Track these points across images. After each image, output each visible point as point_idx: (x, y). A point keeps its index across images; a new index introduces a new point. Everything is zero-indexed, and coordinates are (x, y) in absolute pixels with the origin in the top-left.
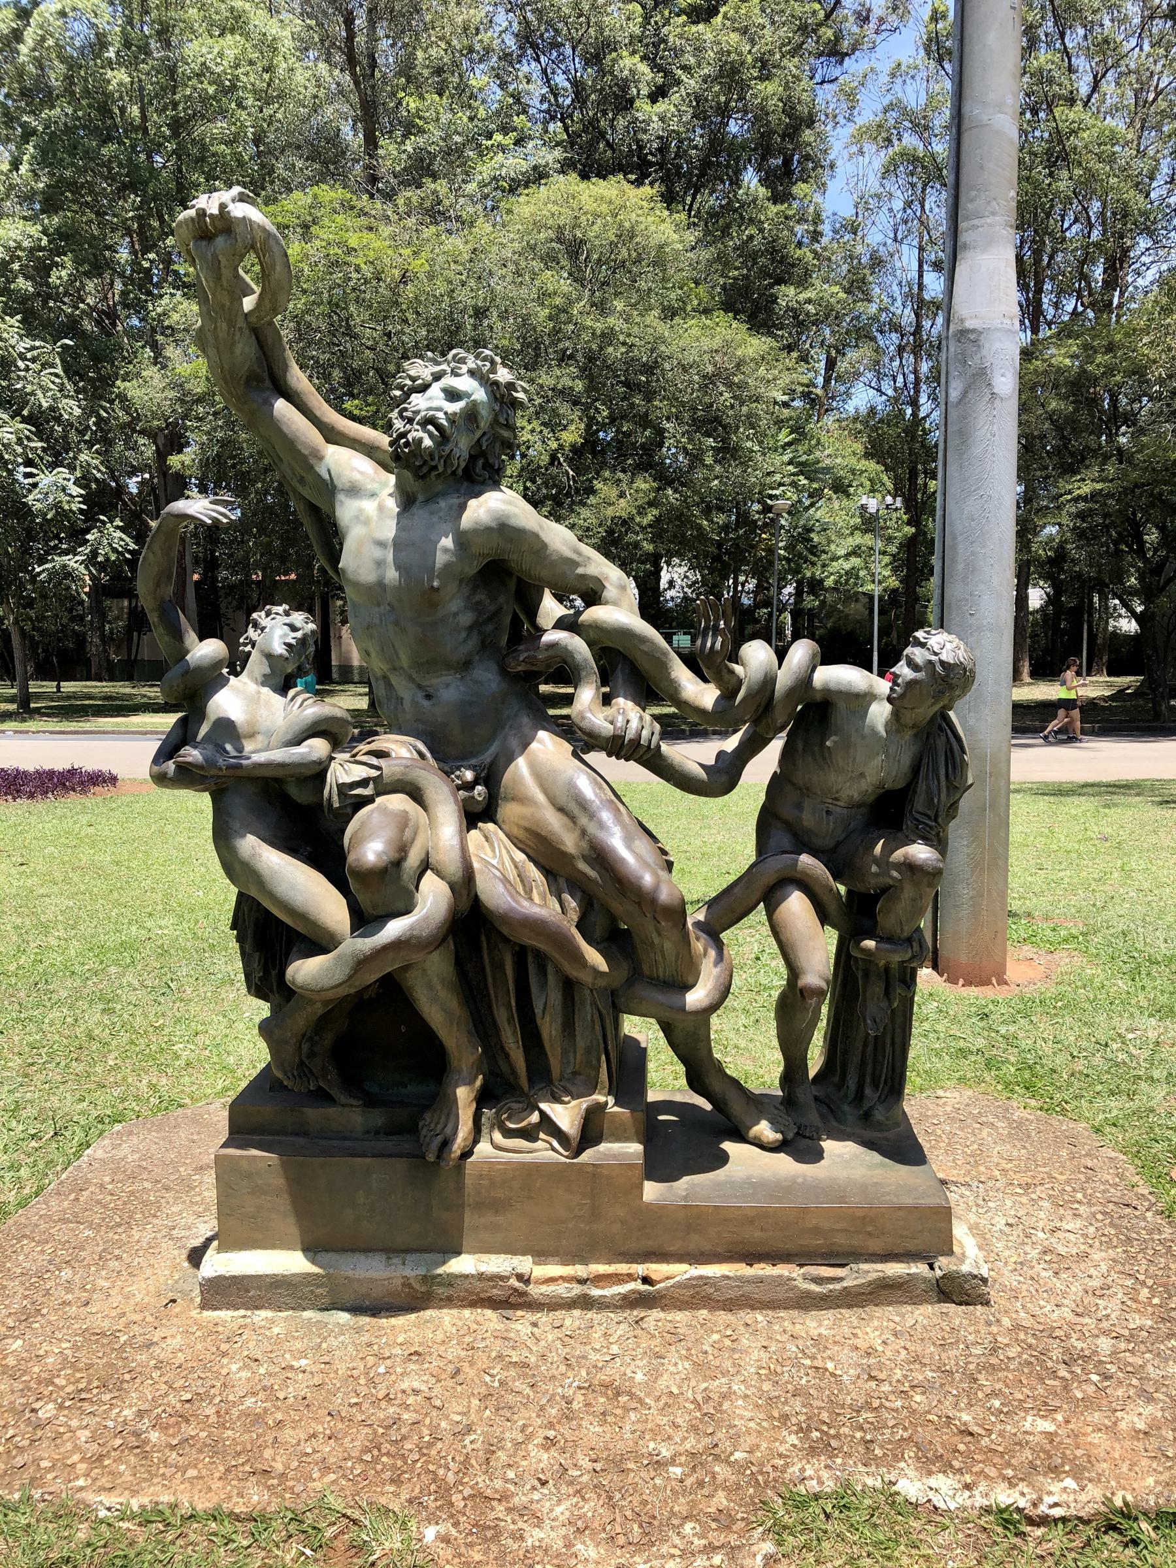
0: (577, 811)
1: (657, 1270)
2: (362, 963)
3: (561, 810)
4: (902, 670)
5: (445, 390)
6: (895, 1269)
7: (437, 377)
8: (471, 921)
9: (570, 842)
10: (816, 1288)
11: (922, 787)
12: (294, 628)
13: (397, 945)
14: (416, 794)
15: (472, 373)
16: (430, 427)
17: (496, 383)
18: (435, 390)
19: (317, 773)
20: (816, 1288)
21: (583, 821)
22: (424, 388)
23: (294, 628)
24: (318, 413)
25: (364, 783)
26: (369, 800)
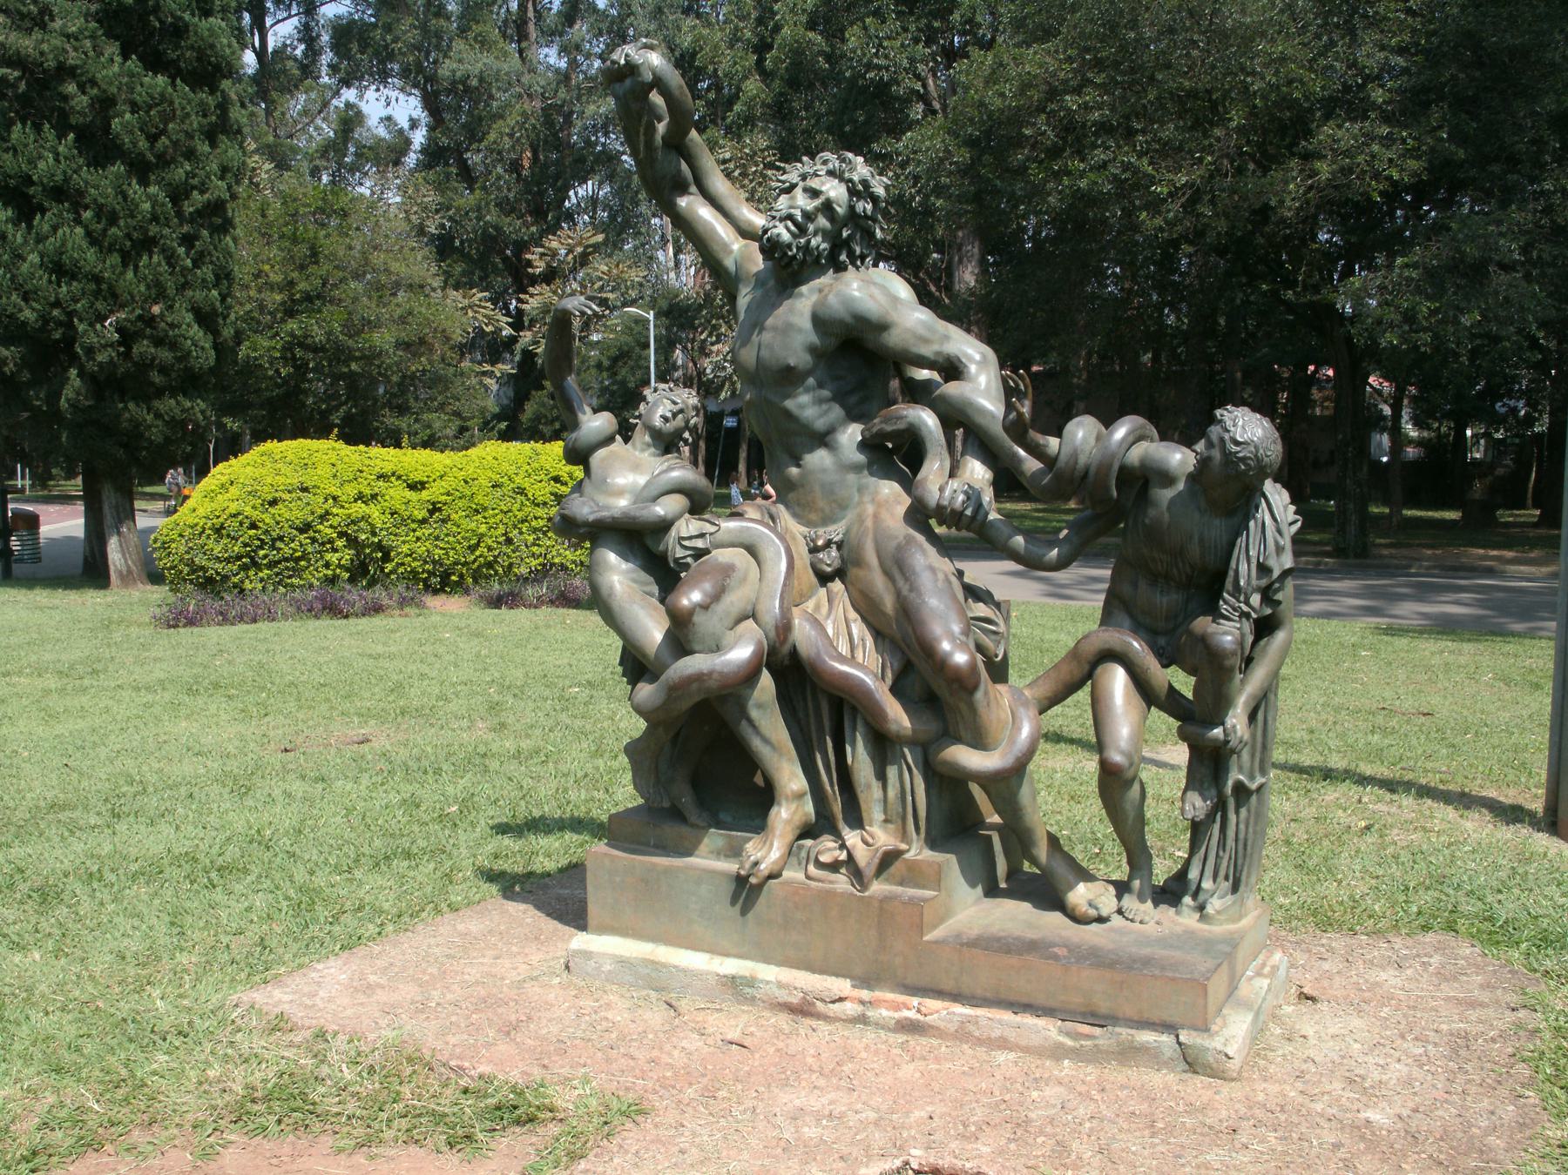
0: (898, 576)
1: (932, 1004)
2: (676, 690)
3: (887, 573)
4: (1200, 446)
5: (805, 190)
6: (1147, 1037)
7: (804, 177)
8: (791, 670)
9: (889, 604)
10: (1069, 1042)
11: (1233, 564)
12: (675, 403)
13: (699, 678)
14: (752, 550)
15: (831, 173)
16: (789, 223)
17: (850, 181)
18: (798, 191)
19: (664, 526)
20: (1069, 1042)
21: (901, 582)
22: (789, 190)
23: (675, 403)
24: (736, 213)
25: (702, 536)
26: (706, 552)
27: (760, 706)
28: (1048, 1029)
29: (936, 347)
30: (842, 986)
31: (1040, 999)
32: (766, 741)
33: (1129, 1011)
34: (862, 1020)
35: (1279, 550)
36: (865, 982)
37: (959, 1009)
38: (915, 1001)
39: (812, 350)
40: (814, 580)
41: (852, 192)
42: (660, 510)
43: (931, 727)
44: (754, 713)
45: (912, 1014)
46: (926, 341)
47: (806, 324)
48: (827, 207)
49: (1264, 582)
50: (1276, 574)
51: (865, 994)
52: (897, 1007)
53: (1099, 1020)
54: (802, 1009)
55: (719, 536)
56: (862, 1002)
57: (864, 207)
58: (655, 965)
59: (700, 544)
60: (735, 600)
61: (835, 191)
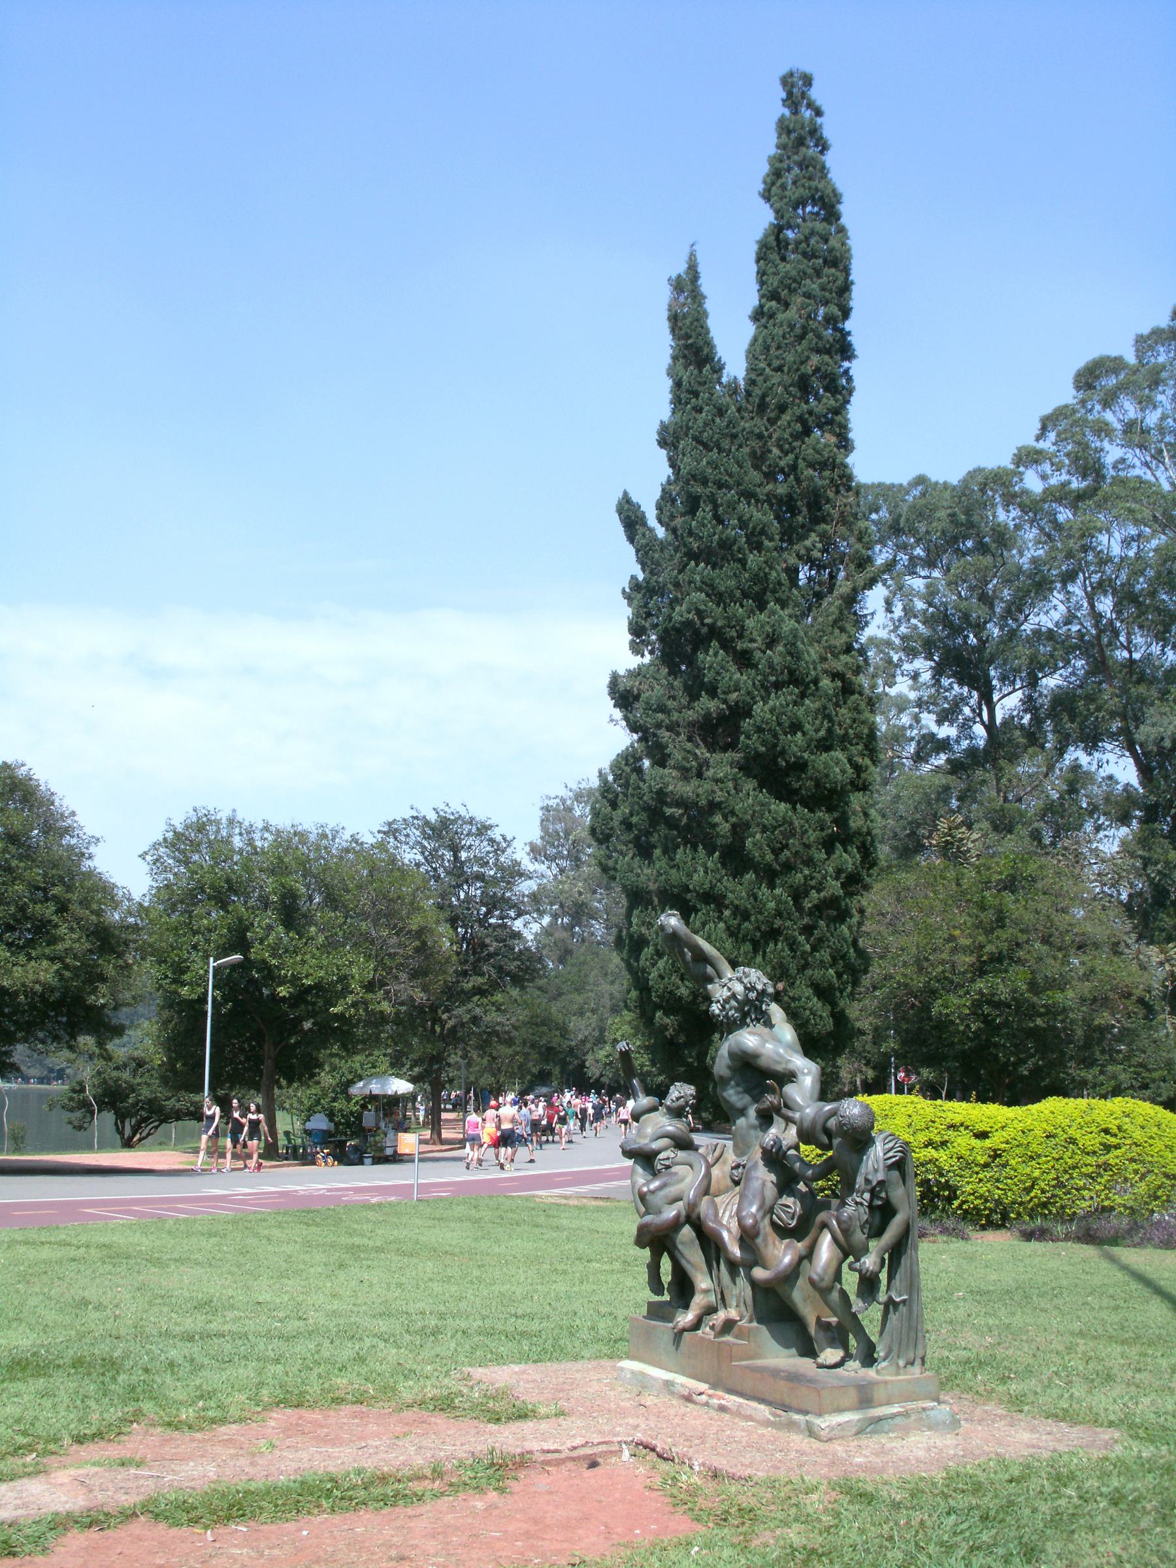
6: (796, 1417)
27: (682, 1243)
28: (764, 1411)
29: (784, 1066)
30: (703, 1387)
31: (767, 1397)
32: (688, 1262)
33: (795, 1404)
34: (707, 1404)
35: (876, 1171)
36: (714, 1386)
37: (741, 1400)
38: (727, 1396)
39: (729, 1067)
40: (729, 1183)
41: (746, 988)
42: (655, 1146)
43: (749, 1257)
44: (680, 1247)
45: (723, 1402)
46: (779, 1063)
47: (726, 1055)
48: (734, 996)
49: (869, 1187)
50: (874, 1183)
51: (711, 1392)
52: (720, 1398)
53: (786, 1408)
54: (688, 1399)
55: (677, 1159)
56: (709, 1396)
57: (752, 995)
58: (643, 1374)
59: (667, 1163)
60: (672, 1190)
61: (739, 988)
